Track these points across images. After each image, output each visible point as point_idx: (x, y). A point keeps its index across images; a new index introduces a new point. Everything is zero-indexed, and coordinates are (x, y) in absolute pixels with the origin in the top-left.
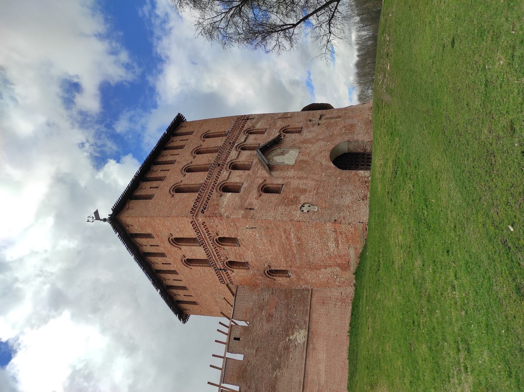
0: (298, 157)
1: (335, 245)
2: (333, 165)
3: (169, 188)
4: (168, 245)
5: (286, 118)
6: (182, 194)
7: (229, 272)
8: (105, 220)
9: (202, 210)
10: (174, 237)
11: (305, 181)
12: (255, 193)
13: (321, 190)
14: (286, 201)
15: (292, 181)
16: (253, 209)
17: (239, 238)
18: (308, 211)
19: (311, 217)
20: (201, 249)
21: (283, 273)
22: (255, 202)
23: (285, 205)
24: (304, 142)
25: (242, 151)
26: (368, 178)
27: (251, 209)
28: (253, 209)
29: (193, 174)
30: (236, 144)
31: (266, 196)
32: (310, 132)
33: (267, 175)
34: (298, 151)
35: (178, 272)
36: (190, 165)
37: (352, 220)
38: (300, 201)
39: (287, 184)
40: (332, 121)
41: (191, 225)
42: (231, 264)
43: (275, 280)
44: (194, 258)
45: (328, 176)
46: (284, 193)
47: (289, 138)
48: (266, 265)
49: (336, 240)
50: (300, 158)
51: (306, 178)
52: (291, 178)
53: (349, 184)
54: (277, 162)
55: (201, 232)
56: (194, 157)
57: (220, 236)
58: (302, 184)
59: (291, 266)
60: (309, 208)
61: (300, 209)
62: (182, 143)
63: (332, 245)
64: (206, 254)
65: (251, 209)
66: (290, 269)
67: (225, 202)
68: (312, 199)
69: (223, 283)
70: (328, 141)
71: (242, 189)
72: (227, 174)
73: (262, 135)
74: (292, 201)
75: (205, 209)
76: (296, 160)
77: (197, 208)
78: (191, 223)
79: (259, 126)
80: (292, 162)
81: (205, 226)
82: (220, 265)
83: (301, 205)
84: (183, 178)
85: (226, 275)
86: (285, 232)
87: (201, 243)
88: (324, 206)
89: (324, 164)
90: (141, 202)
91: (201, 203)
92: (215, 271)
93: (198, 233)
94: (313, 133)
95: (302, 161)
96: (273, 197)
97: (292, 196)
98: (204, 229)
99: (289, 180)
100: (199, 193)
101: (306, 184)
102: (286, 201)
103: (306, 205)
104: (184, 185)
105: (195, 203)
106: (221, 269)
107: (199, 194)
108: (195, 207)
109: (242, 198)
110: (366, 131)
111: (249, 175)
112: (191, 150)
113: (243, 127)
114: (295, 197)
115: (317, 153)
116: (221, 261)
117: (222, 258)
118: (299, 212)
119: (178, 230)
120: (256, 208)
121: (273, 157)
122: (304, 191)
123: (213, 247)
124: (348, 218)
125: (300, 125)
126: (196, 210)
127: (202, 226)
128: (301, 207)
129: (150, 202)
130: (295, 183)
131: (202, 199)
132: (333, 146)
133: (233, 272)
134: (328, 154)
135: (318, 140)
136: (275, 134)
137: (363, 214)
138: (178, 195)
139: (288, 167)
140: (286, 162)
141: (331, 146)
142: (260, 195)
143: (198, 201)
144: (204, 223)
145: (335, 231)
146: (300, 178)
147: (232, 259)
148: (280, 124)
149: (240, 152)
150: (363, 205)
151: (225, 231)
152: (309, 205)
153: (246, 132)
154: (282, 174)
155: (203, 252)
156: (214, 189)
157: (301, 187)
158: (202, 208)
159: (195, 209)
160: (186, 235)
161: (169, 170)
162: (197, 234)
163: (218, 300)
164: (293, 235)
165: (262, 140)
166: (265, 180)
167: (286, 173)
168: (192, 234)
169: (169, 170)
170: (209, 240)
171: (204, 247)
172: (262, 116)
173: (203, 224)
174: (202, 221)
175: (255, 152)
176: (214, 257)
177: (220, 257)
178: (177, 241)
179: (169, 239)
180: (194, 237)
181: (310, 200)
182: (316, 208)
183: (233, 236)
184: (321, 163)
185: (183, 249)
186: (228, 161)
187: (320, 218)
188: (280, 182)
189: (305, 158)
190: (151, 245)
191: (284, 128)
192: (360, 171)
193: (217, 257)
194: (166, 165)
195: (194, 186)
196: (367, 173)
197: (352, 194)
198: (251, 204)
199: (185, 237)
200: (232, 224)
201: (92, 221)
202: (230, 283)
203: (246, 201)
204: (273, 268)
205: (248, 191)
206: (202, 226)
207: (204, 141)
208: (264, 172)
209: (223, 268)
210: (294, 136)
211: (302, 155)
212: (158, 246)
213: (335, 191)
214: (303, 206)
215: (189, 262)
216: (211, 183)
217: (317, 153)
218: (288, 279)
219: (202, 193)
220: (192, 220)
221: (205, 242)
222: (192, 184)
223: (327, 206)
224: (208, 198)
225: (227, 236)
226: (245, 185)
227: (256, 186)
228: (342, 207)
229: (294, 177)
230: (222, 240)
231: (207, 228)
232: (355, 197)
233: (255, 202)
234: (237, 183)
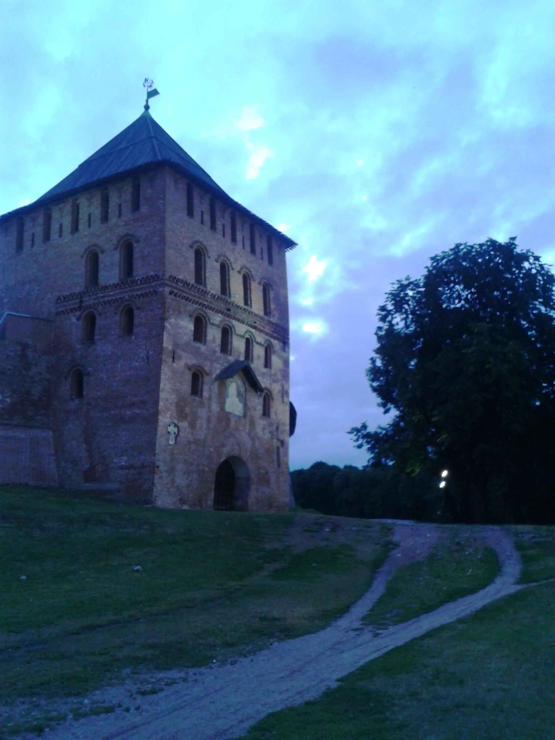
0: (235, 416)
1: (122, 465)
2: (222, 460)
3: (201, 239)
4: (121, 231)
6: (194, 260)
7: (78, 313)
8: (147, 107)
9: (173, 292)
10: (135, 245)
11: (204, 426)
12: (192, 361)
13: (193, 447)
14: (182, 403)
16: (173, 361)
17: (133, 337)
18: (169, 433)
20: (115, 280)
21: (79, 392)
23: (177, 403)
24: (252, 423)
25: (244, 340)
27: (174, 358)
28: (173, 361)
29: (218, 273)
30: (253, 331)
31: (188, 377)
32: (264, 429)
33: (214, 376)
35: (76, 235)
36: (230, 268)
38: (182, 421)
39: (202, 404)
40: (275, 457)
41: (152, 273)
42: (91, 321)
43: (66, 378)
44: (101, 266)
47: (256, 402)
48: (90, 369)
49: (130, 467)
51: (208, 428)
55: (142, 286)
56: (239, 272)
57: (136, 313)
58: (201, 423)
59: (89, 404)
60: (172, 433)
62: (258, 250)
64: (108, 284)
66: (86, 401)
69: (57, 300)
71: (198, 345)
72: (217, 322)
73: (263, 366)
75: (175, 295)
76: (229, 413)
77: (176, 284)
78: (156, 275)
79: (276, 360)
80: (228, 408)
81: (152, 294)
82: (89, 301)
83: (176, 423)
84: (213, 258)
85: (72, 307)
87: (124, 281)
90: (183, 202)
91: (182, 288)
92: (79, 293)
93: (141, 281)
94: (261, 433)
95: (229, 420)
96: (187, 387)
97: (188, 410)
98: (147, 291)
100: (195, 285)
101: (201, 427)
102: (182, 403)
103: (176, 430)
104: (205, 261)
105: (182, 281)
106: (81, 302)
107: (193, 285)
108: (177, 281)
109: (187, 344)
111: (214, 352)
112: (249, 265)
113: (275, 338)
114: (186, 415)
116: (96, 306)
117: (100, 308)
119: (146, 253)
120: (175, 365)
122: (193, 426)
123: (118, 297)
125: (273, 415)
126: (174, 282)
127: (151, 290)
128: (174, 423)
129: (183, 214)
130: (203, 413)
131: (187, 290)
132: (244, 459)
133: (78, 319)
134: (236, 453)
135: (253, 440)
136: (264, 382)
138: (191, 255)
139: (222, 403)
140: (228, 401)
141: (245, 456)
142: (190, 369)
143: (184, 285)
144: (157, 294)
145: (143, 467)
146: (209, 420)
147: (100, 322)
148: (276, 388)
149: (244, 338)
151: (144, 321)
152: (176, 432)
153: (268, 342)
155: (111, 282)
156: (199, 305)
157: (198, 422)
158: (176, 291)
159: (175, 281)
160: (137, 264)
161: (224, 236)
162: (138, 279)
163: (27, 287)
164: (138, 412)
165: (257, 365)
166: (208, 374)
168: (140, 272)
169: (224, 236)
171: (118, 284)
172: (286, 363)
173: (154, 291)
174: (159, 291)
175: (242, 358)
179: (131, 235)
180: (135, 274)
181: (182, 434)
183: (135, 330)
184: (224, 446)
185: (114, 252)
186: (234, 322)
188: (205, 394)
189: (233, 424)
190: (120, 206)
192: (213, 494)
194: (230, 232)
195: (203, 276)
196: (210, 503)
197: (188, 486)
198: (180, 357)
199: (135, 262)
200: (154, 333)
201: (145, 84)
202: (58, 312)
203: (183, 350)
204: (85, 378)
205: (197, 353)
207: (260, 283)
208: (218, 372)
209: (84, 305)
210: (260, 408)
212: (120, 215)
214: (176, 425)
216: (207, 301)
218: (68, 398)
219: (195, 289)
220: (160, 277)
221: (127, 288)
222: (205, 274)
224: (188, 298)
225: (136, 321)
226: (203, 348)
229: (210, 411)
230: (130, 314)
231: (148, 296)
234: (206, 336)
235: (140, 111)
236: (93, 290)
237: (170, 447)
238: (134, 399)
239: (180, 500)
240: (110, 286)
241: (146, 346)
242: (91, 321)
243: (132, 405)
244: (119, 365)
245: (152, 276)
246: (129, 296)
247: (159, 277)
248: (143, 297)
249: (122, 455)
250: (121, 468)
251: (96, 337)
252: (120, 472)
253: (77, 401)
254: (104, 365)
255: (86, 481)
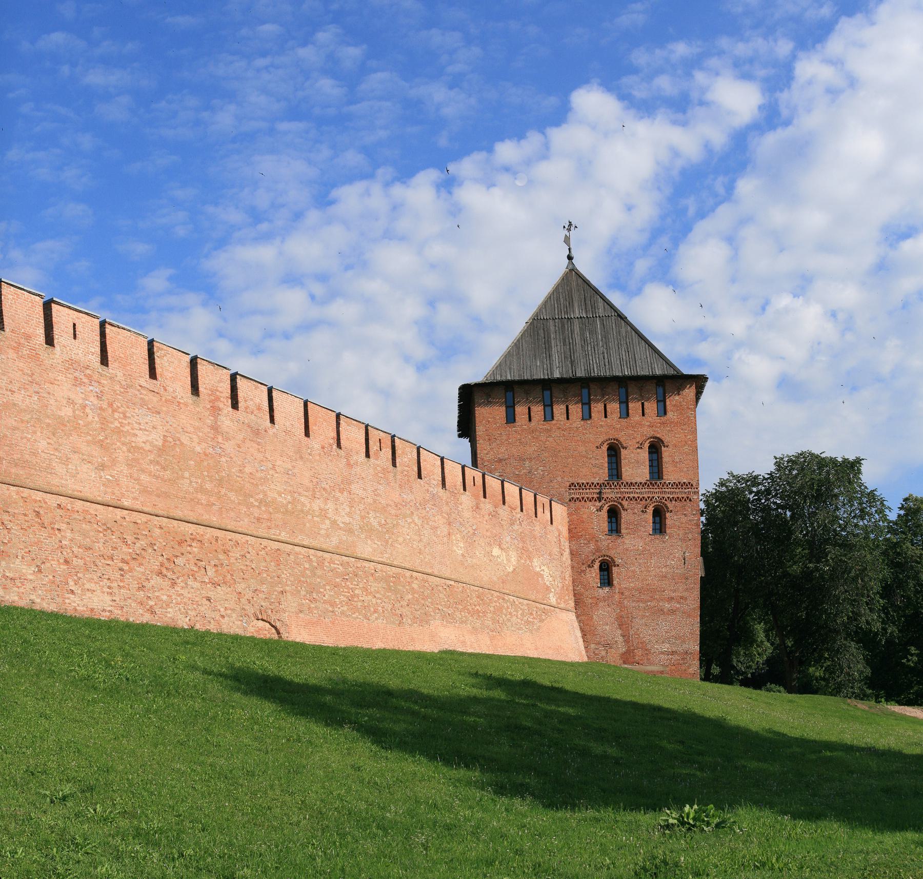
41: (685, 481)
49: (673, 653)
59: (622, 593)
63: (666, 647)
64: (634, 481)
69: (570, 486)
85: (590, 496)
86: (682, 598)
144: (690, 500)
155: (639, 480)
162: (669, 483)
170: (661, 496)
173: (688, 498)
176: (626, 490)
177: (626, 500)
178: (655, 448)
183: (668, 531)
193: (627, 496)
206: (685, 496)
215: (614, 451)
235: (562, 266)
236: (615, 483)
238: (673, 595)
240: (636, 483)
241: (682, 547)
242: (614, 514)
243: (671, 599)
244: (653, 561)
245: (684, 483)
246: (658, 497)
247: (692, 485)
248: (676, 500)
249: (663, 642)
250: (662, 653)
251: (623, 531)
252: (662, 656)
253: (607, 589)
254: (636, 559)
255: (625, 663)
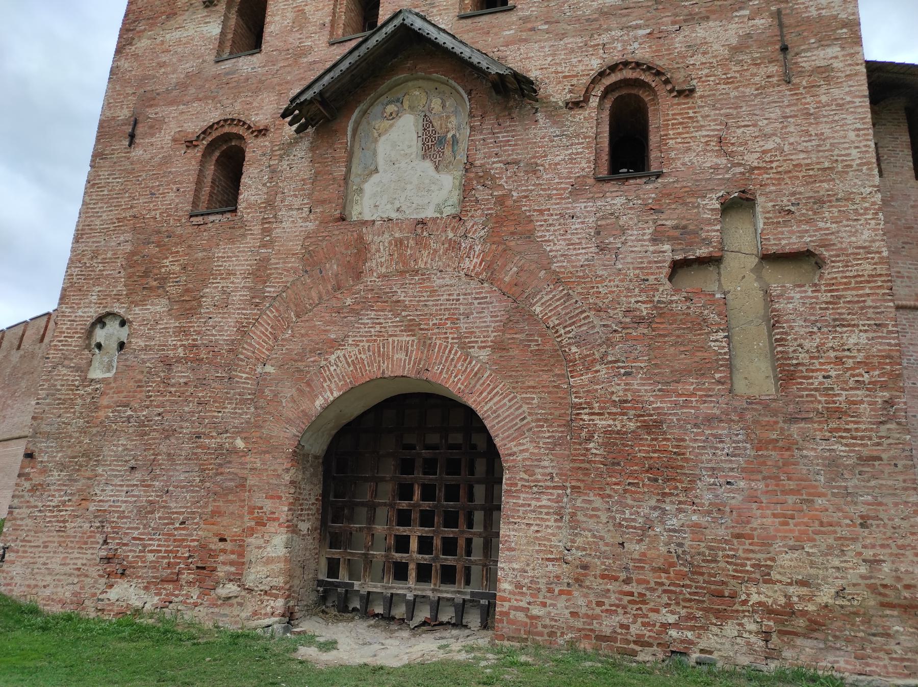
5: (784, 49)
14: (152, 249)
15: (251, 241)
16: (130, 145)
19: (66, 362)
22: (164, 138)
26: (236, 578)
34: (448, 211)
37: (22, 519)
38: (142, 303)
39: (236, 232)
45: (258, 393)
46: (190, 230)
50: (377, 239)
51: (256, 299)
52: (266, 231)
53: (203, 493)
54: (376, 141)
61: (109, 314)
65: (132, 136)
67: (177, 34)
68: (146, 349)
70: (499, 347)
74: (146, 274)
88: (105, 401)
89: (332, 358)
94: (585, 253)
95: (362, 250)
99: (257, 229)
102: (152, 249)
110: (598, 565)
115: (406, 308)
118: (93, 312)
120: (138, 153)
121: (412, 108)
124: (33, 504)
137: (42, 560)
142: (190, 144)
150: (79, 562)
154: (288, 188)
157: (212, 294)
166: (262, 132)
167: (297, 202)
182: (109, 371)
184: (336, 344)
187: (53, 395)
191: (659, 73)
197: (145, 511)
198: (157, 125)
203: (172, 103)
211: (399, 243)
213: (169, 433)
217: (406, 308)
223: (102, 414)
227: (235, 109)
228: (89, 474)
232: (125, 524)
233: (164, 138)
237: (89, 389)
239: (108, 560)
